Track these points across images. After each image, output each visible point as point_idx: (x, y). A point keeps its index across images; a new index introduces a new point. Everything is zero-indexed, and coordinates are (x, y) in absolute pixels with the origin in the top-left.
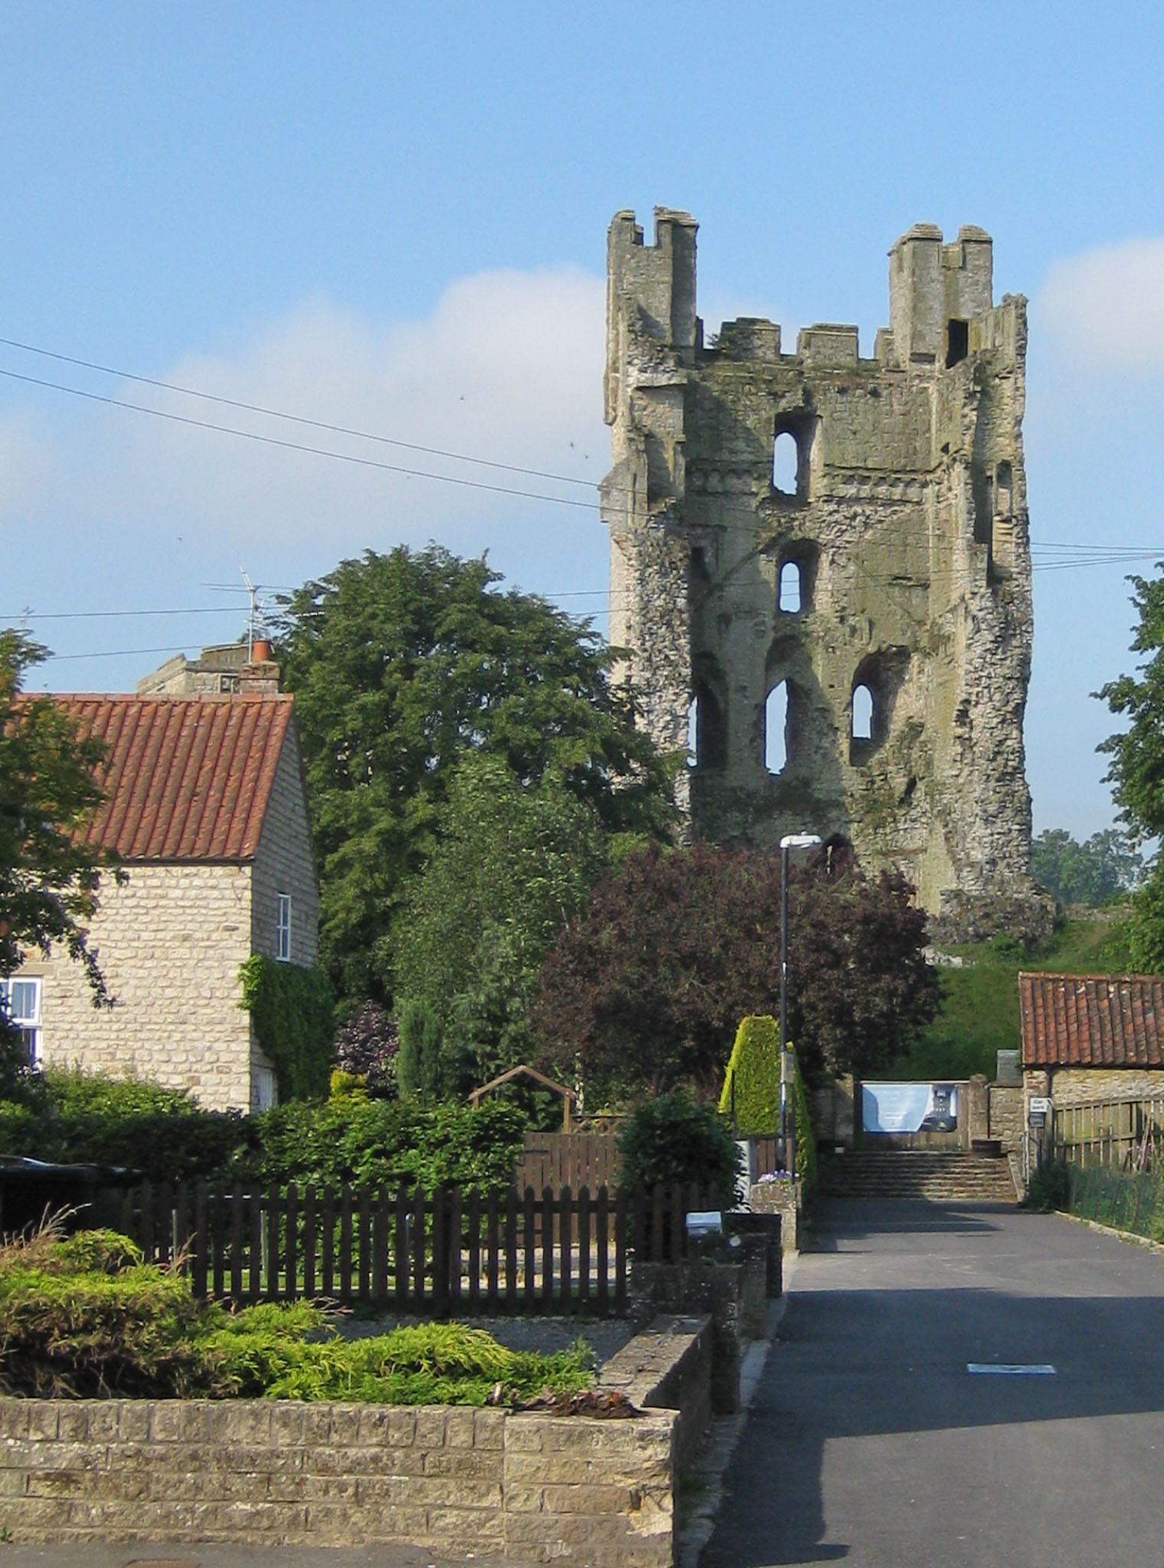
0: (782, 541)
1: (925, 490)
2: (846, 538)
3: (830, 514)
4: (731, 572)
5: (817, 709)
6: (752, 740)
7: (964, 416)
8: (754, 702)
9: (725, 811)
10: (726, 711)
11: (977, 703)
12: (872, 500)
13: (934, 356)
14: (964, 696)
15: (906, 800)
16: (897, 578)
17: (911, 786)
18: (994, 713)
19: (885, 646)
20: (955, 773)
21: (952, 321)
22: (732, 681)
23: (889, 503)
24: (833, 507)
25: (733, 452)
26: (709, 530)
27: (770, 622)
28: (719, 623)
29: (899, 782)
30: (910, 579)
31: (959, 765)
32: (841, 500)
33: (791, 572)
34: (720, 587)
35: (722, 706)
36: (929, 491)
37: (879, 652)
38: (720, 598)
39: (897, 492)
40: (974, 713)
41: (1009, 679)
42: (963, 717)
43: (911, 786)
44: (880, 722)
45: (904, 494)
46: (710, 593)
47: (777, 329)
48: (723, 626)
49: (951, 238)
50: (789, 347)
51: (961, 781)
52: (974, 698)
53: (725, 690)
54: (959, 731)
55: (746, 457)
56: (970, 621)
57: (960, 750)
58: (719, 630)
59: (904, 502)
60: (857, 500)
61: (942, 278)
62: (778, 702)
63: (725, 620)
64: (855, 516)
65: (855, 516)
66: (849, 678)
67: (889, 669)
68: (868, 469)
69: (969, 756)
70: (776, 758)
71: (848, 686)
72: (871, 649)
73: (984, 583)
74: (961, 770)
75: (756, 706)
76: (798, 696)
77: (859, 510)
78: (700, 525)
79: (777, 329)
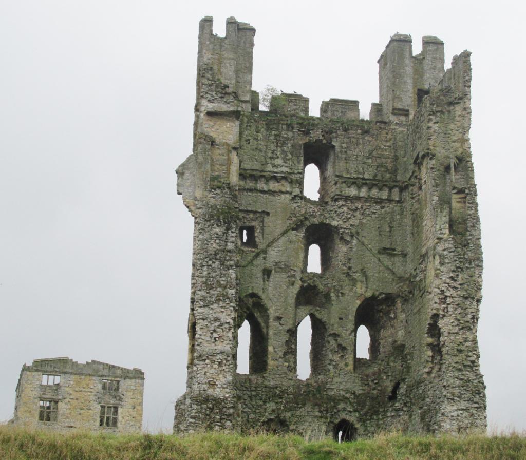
0: (307, 223)
1: (404, 193)
2: (351, 222)
3: (339, 208)
4: (272, 242)
5: (330, 335)
6: (285, 354)
7: (429, 128)
8: (287, 328)
9: (265, 402)
10: (267, 334)
11: (444, 316)
12: (367, 199)
13: (408, 111)
14: (435, 311)
15: (393, 397)
16: (385, 249)
17: (396, 387)
18: (456, 323)
19: (377, 293)
20: (427, 370)
21: (419, 90)
22: (272, 312)
23: (379, 201)
24: (341, 203)
25: (274, 166)
26: (258, 215)
27: (299, 275)
28: (264, 275)
29: (389, 385)
30: (394, 250)
31: (430, 365)
32: (347, 198)
33: (315, 251)
34: (265, 252)
35: (264, 330)
36: (406, 194)
37: (373, 298)
38: (265, 258)
39: (384, 195)
40: (441, 323)
41: (466, 298)
42: (434, 330)
43: (396, 387)
44: (374, 348)
45: (389, 196)
46: (257, 255)
47: (306, 101)
48: (265, 276)
49: (417, 48)
50: (315, 111)
51: (433, 375)
52: (441, 312)
53: (266, 317)
54: (430, 340)
55: (284, 169)
56: (437, 257)
57: (430, 353)
58: (264, 281)
59: (390, 200)
60: (358, 198)
61: (412, 64)
62: (305, 330)
63: (267, 273)
64: (356, 209)
65: (356, 209)
66: (352, 318)
67: (381, 311)
68: (363, 179)
69: (439, 358)
70: (304, 370)
71: (351, 326)
72: (369, 294)
73: (447, 231)
74: (432, 368)
75: (288, 331)
76: (318, 327)
77: (359, 206)
78: (251, 212)
79: (306, 101)
